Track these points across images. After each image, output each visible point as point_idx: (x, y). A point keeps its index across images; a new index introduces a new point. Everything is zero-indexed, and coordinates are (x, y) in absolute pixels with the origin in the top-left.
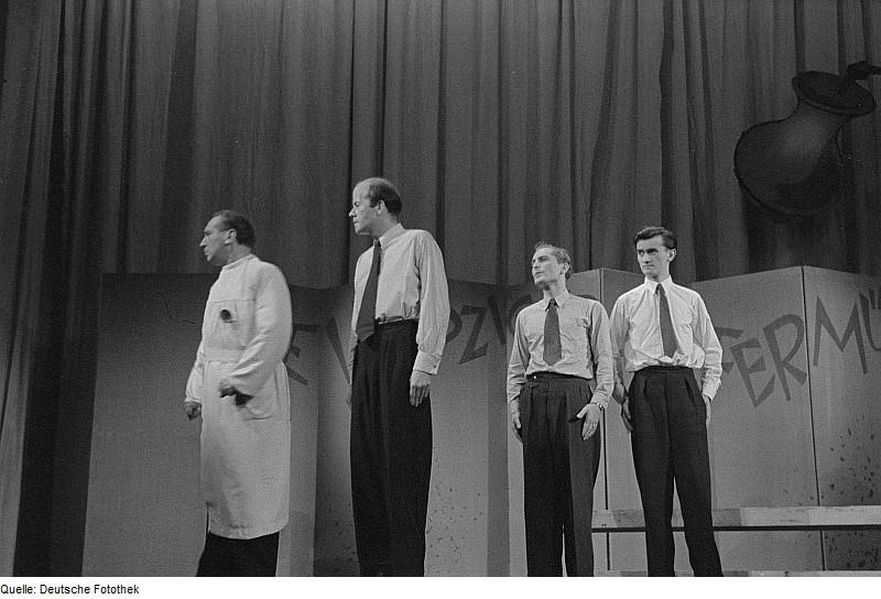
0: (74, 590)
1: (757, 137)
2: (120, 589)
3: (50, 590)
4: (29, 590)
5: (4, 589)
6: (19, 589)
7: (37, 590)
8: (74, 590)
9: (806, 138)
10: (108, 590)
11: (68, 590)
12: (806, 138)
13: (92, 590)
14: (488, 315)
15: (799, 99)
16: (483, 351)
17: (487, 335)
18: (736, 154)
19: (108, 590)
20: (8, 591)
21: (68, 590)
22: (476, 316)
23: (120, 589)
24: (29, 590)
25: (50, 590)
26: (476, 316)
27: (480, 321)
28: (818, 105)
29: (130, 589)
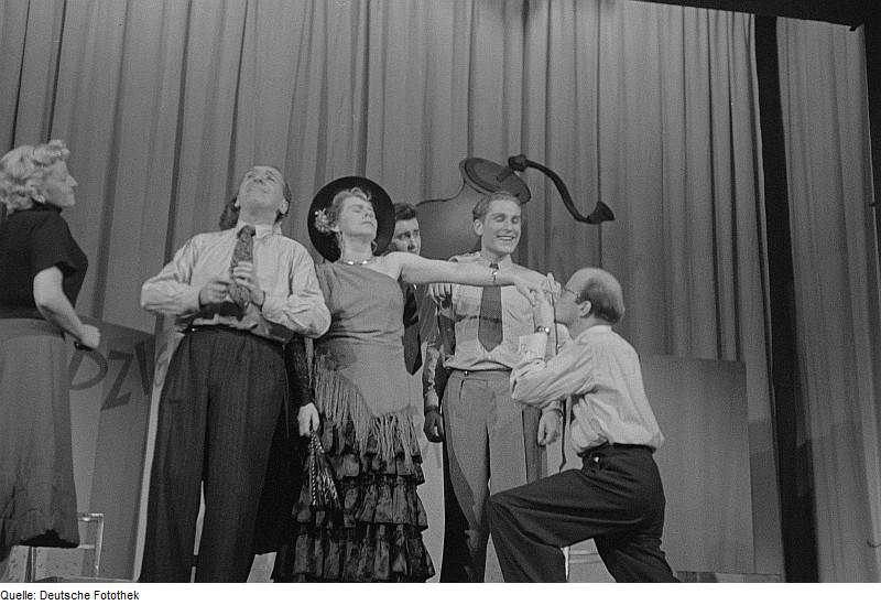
0: (74, 596)
2: (120, 595)
3: (50, 596)
4: (29, 596)
5: (4, 595)
6: (19, 595)
7: (37, 596)
8: (74, 596)
10: (108, 596)
11: (68, 596)
13: (92, 595)
14: (135, 361)
15: (465, 182)
16: (125, 400)
17: (132, 384)
19: (108, 596)
21: (68, 596)
22: (122, 363)
23: (120, 595)
24: (29, 596)
25: (50, 596)
26: (122, 363)
27: (126, 368)
28: (482, 190)
29: (130, 594)
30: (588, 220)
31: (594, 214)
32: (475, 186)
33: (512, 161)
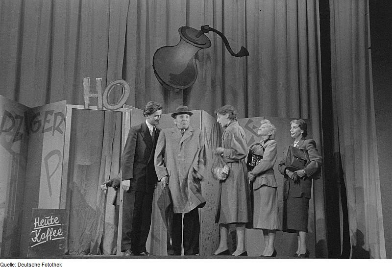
0: (33, 265)
1: (164, 52)
2: (53, 265)
3: (22, 265)
4: (13, 265)
5: (2, 265)
6: (8, 264)
7: (17, 265)
8: (33, 265)
9: (185, 54)
10: (48, 265)
11: (30, 265)
12: (185, 54)
13: (41, 264)
15: (181, 38)
18: (154, 58)
20: (3, 265)
21: (30, 265)
23: (53, 265)
24: (13, 265)
25: (22, 265)
28: (189, 42)
29: (58, 264)
30: (237, 56)
31: (240, 52)
32: (186, 40)
33: (202, 27)
